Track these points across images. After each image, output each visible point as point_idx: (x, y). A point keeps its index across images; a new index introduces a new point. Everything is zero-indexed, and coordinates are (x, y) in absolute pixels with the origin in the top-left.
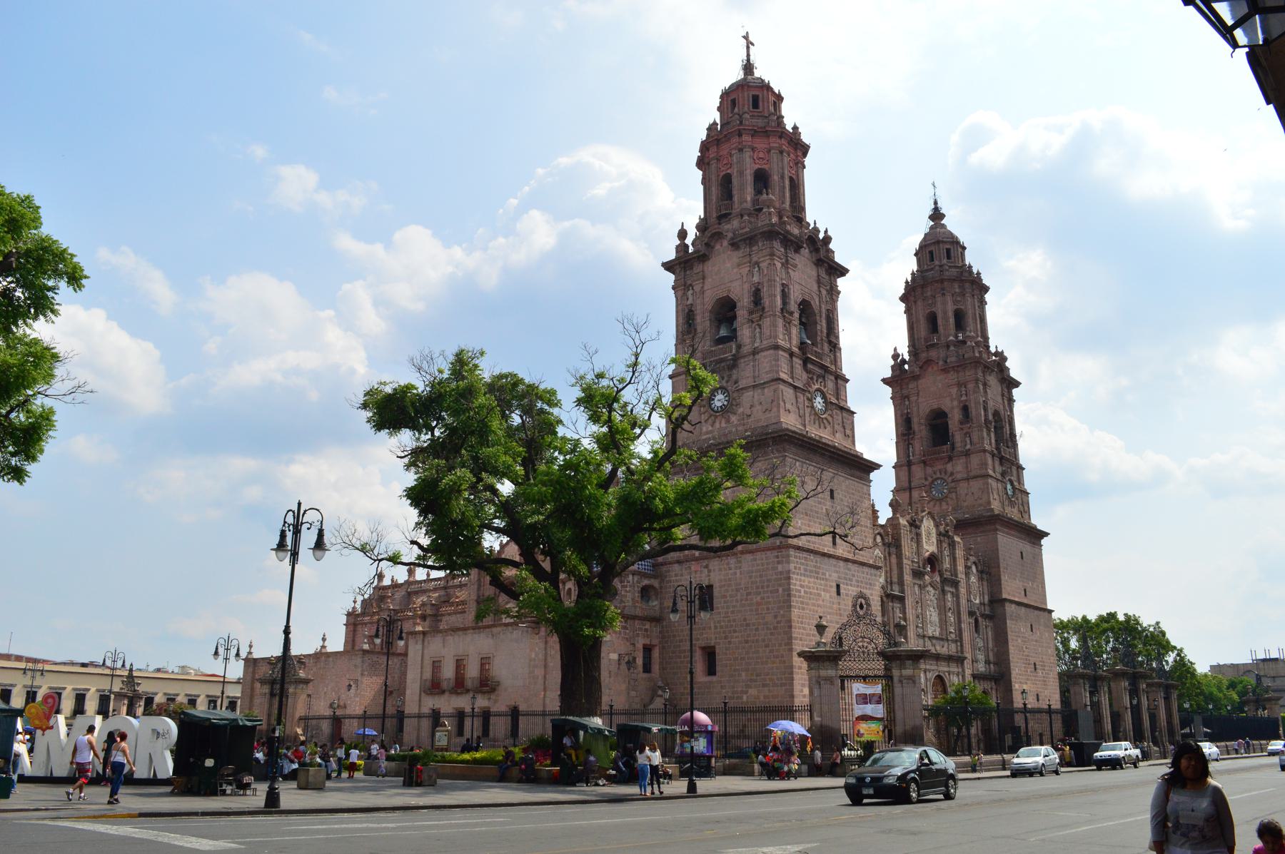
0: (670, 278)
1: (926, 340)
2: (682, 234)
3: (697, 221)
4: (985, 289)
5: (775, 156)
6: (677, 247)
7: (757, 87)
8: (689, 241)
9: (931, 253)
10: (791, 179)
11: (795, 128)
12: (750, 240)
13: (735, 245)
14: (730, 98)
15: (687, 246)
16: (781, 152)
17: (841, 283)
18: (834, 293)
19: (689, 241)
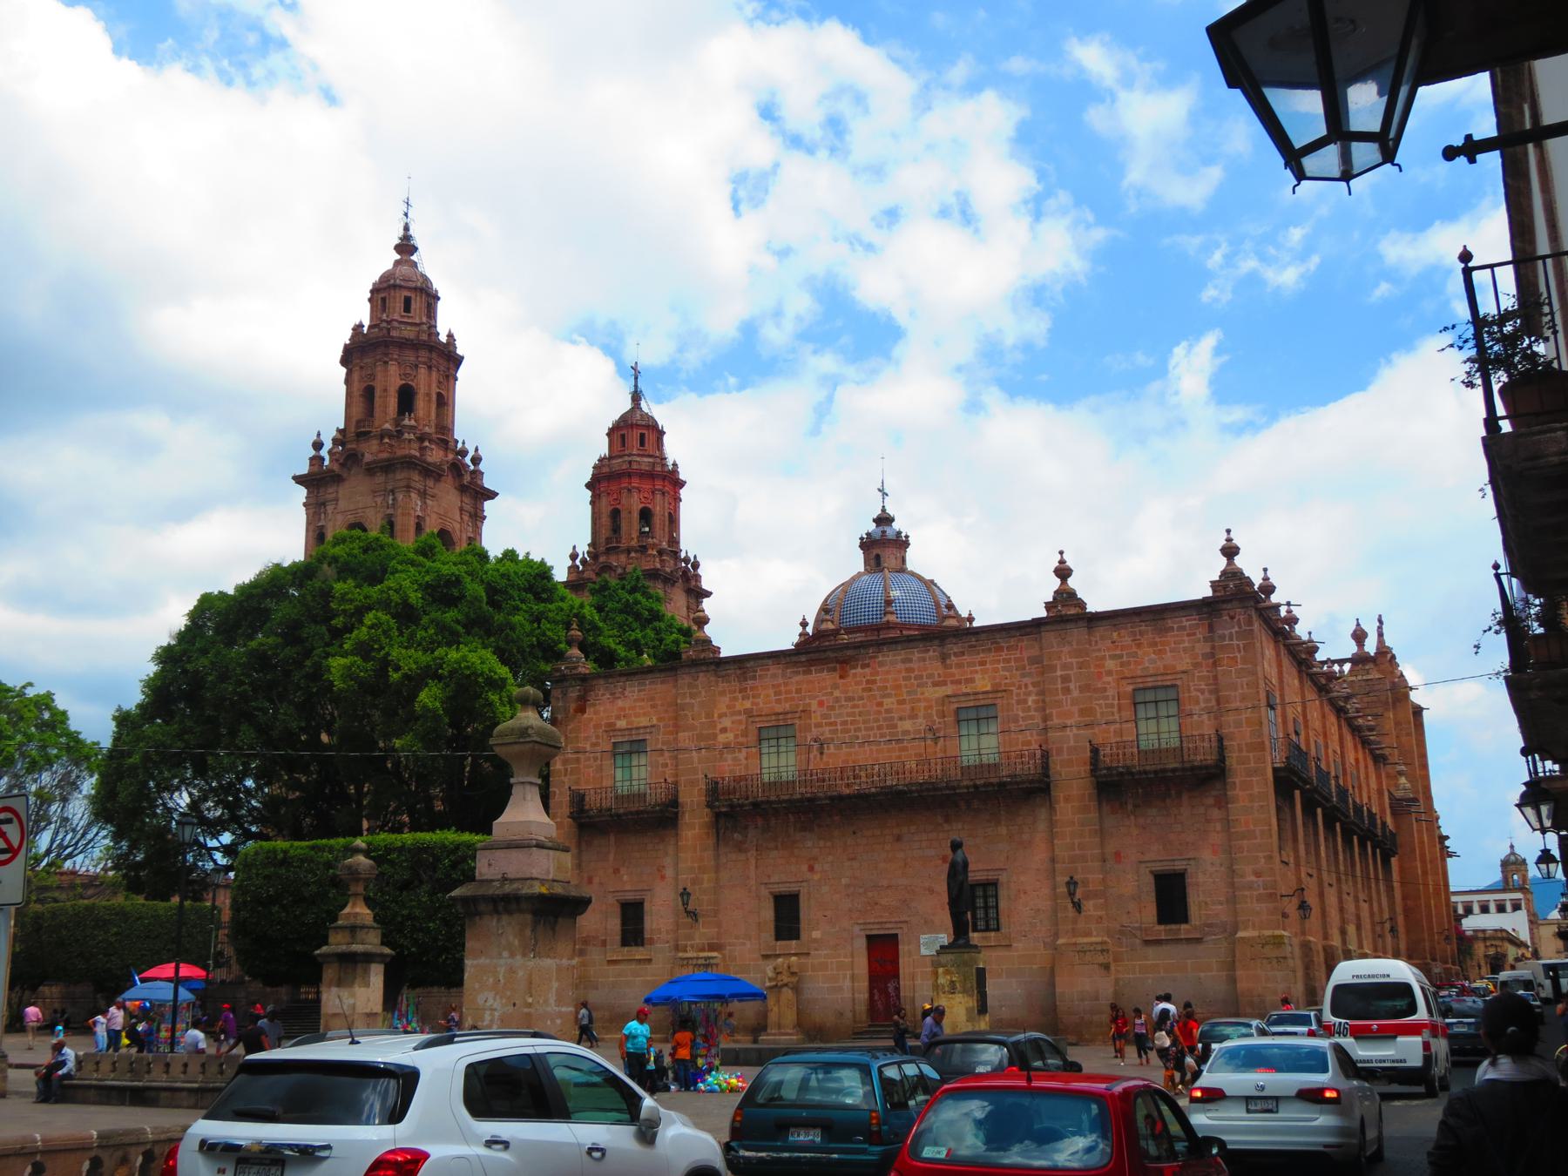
0: (301, 493)
1: (608, 540)
2: (318, 445)
3: (334, 433)
4: (682, 484)
5: (423, 371)
6: (311, 459)
7: (409, 289)
8: (324, 452)
9: (623, 436)
10: (439, 395)
11: (450, 336)
12: (387, 467)
13: (371, 470)
14: (382, 293)
15: (323, 459)
16: (430, 368)
17: (488, 506)
18: (478, 517)
19: (324, 452)
